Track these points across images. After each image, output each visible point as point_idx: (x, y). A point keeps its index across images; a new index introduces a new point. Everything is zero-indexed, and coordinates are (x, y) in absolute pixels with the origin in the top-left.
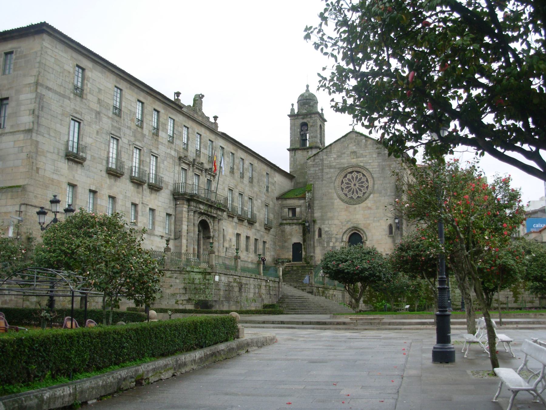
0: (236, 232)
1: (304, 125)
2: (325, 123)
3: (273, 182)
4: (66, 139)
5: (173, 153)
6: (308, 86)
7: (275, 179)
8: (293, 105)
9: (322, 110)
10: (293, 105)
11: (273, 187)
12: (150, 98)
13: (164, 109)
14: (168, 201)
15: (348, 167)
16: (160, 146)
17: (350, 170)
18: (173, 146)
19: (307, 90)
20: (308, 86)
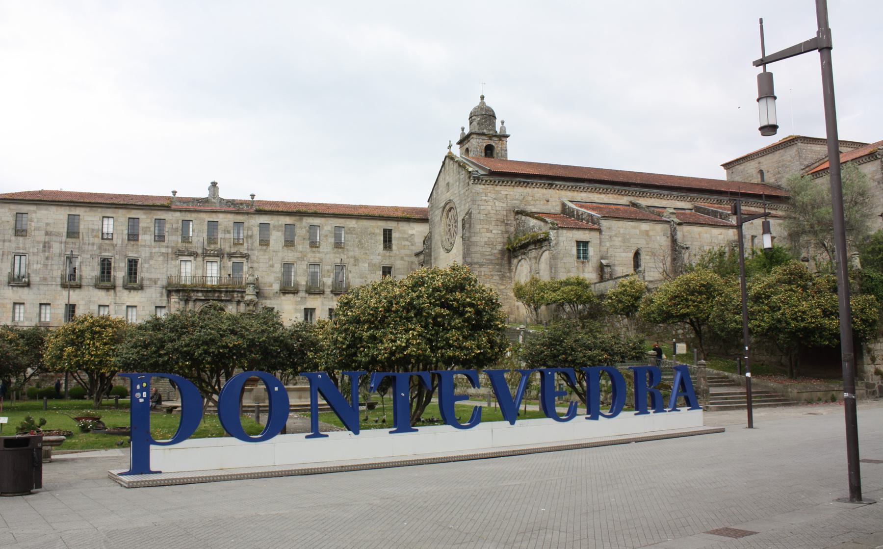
0: (303, 307)
1: (467, 150)
2: (508, 139)
3: (406, 236)
4: (10, 271)
5: (164, 250)
6: (482, 98)
7: (410, 232)
8: (463, 129)
9: (503, 123)
10: (463, 129)
11: (407, 243)
12: (120, 211)
13: (145, 214)
14: (158, 295)
15: (446, 204)
16: (141, 249)
17: (448, 207)
18: (164, 244)
19: (483, 103)
20: (482, 98)
